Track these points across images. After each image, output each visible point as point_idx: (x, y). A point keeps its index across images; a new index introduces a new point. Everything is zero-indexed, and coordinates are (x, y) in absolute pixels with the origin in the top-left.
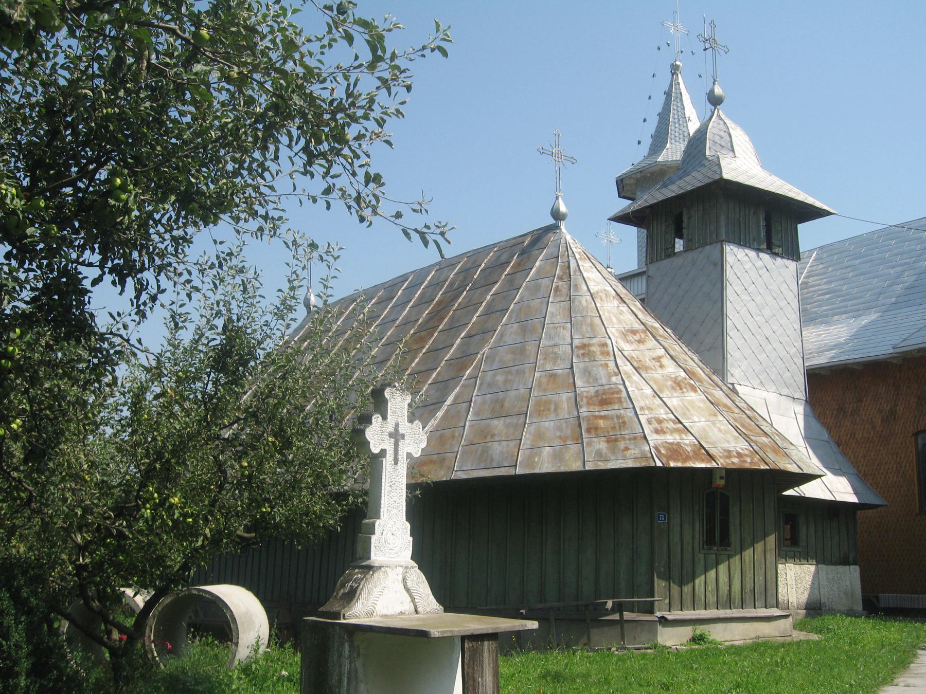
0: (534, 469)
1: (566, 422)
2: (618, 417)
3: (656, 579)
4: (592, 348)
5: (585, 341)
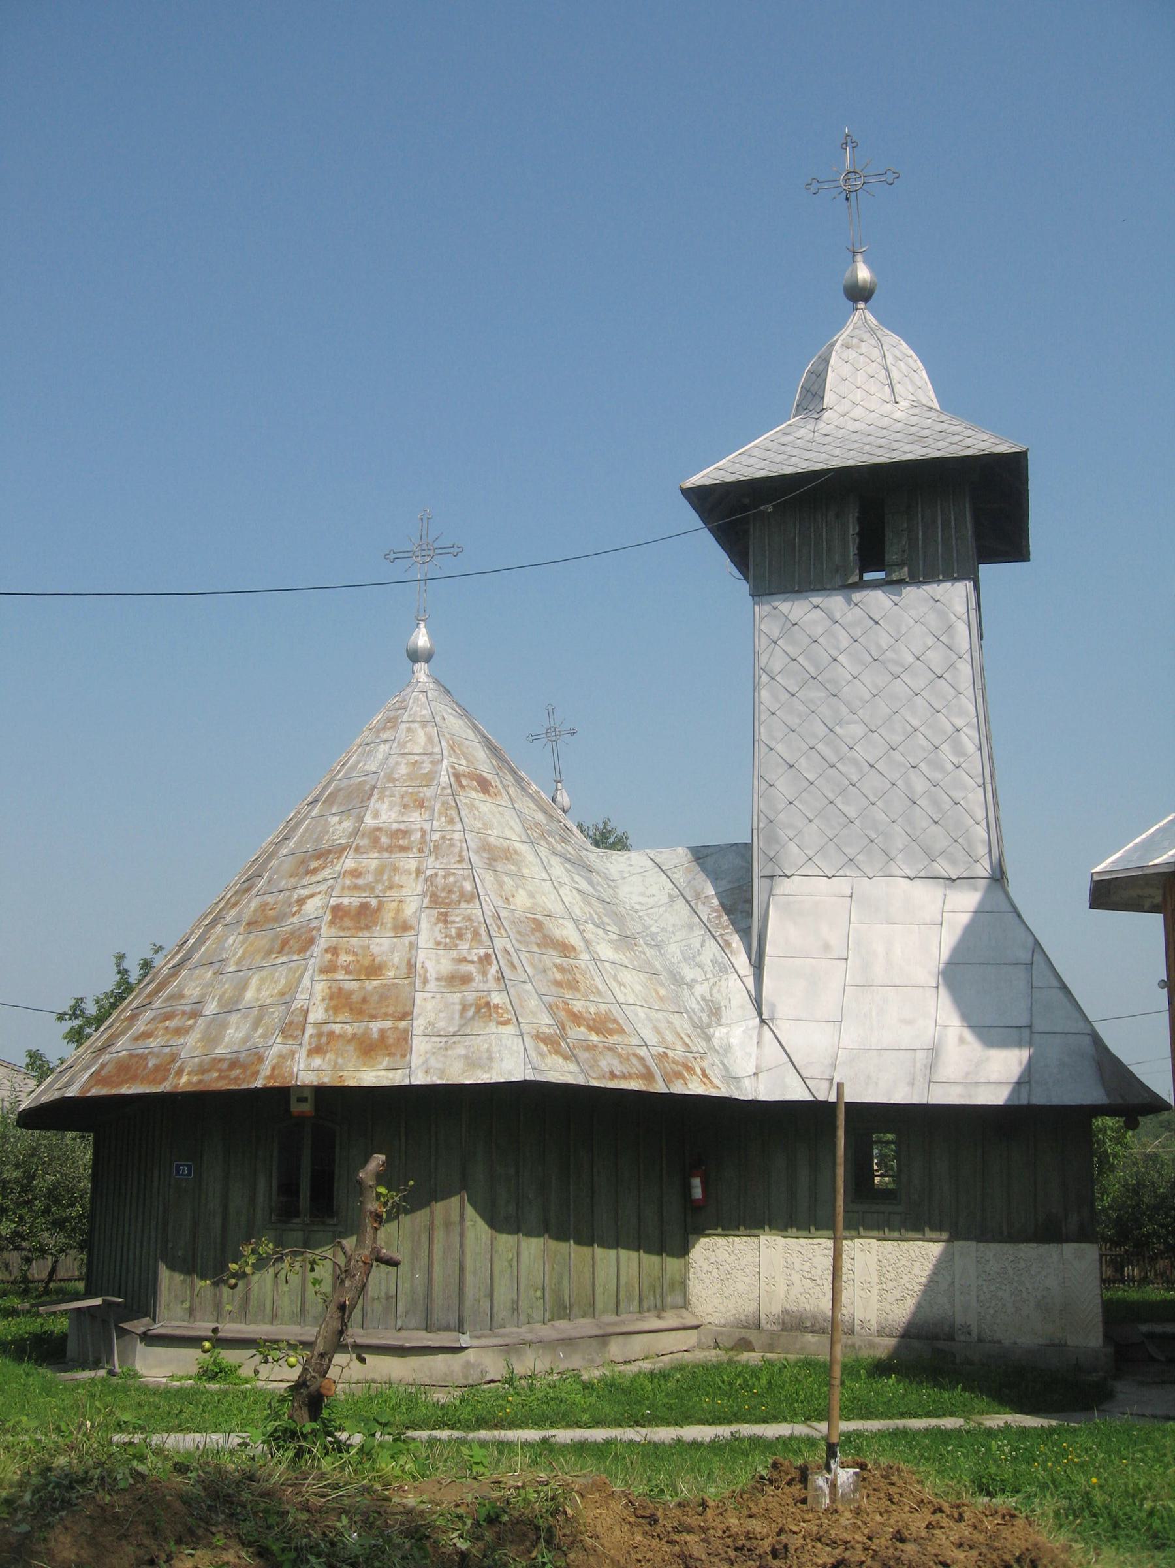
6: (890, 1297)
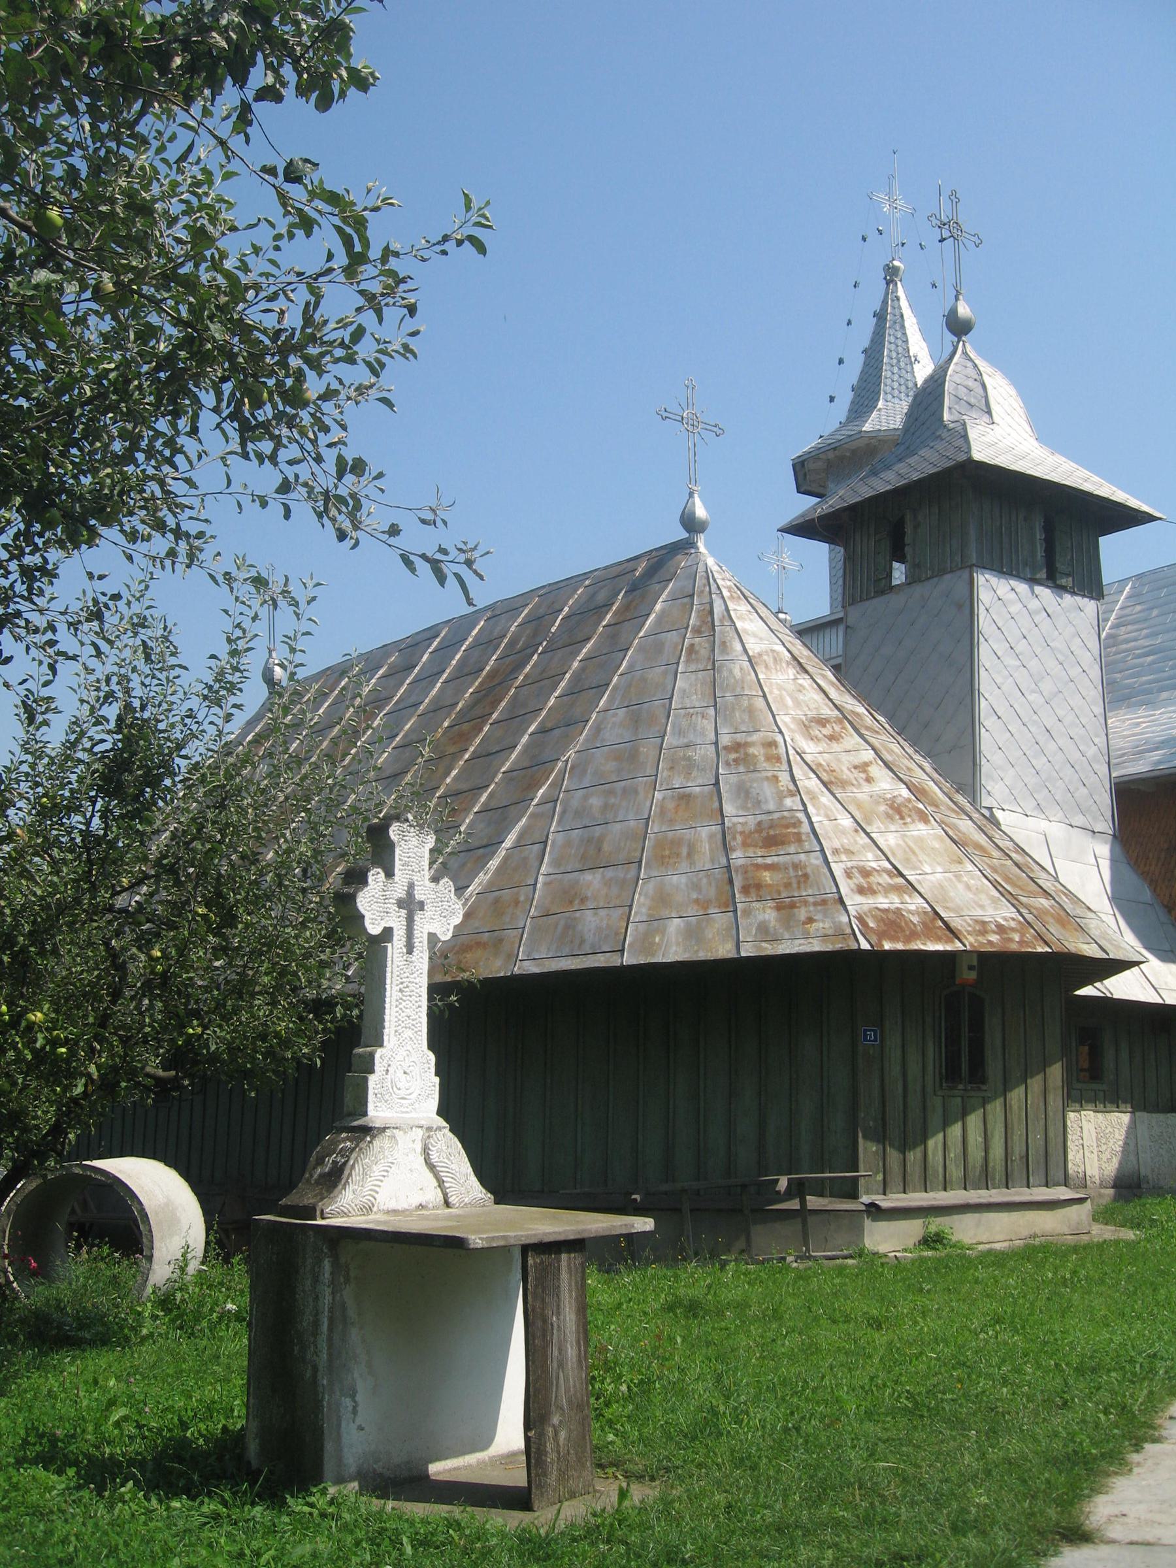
0: (653, 955)
1: (707, 876)
2: (796, 866)
3: (861, 1140)
4: (752, 750)
5: (740, 738)
6: (1105, 1159)
